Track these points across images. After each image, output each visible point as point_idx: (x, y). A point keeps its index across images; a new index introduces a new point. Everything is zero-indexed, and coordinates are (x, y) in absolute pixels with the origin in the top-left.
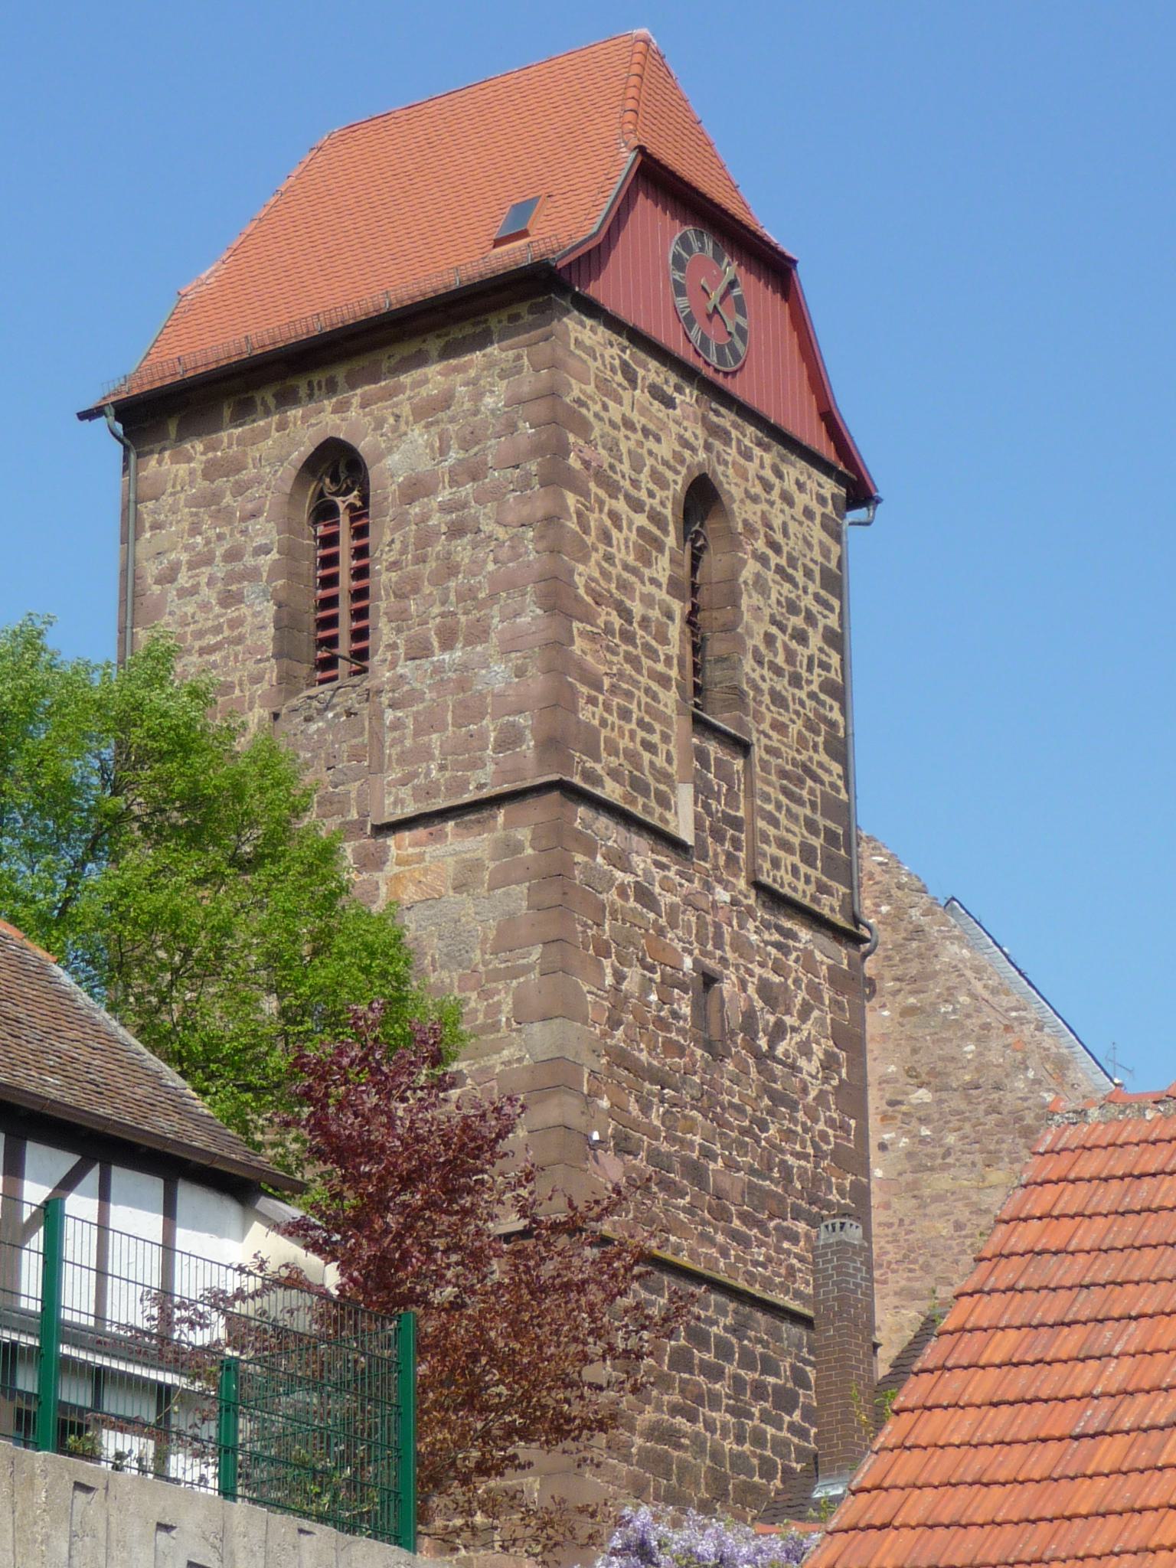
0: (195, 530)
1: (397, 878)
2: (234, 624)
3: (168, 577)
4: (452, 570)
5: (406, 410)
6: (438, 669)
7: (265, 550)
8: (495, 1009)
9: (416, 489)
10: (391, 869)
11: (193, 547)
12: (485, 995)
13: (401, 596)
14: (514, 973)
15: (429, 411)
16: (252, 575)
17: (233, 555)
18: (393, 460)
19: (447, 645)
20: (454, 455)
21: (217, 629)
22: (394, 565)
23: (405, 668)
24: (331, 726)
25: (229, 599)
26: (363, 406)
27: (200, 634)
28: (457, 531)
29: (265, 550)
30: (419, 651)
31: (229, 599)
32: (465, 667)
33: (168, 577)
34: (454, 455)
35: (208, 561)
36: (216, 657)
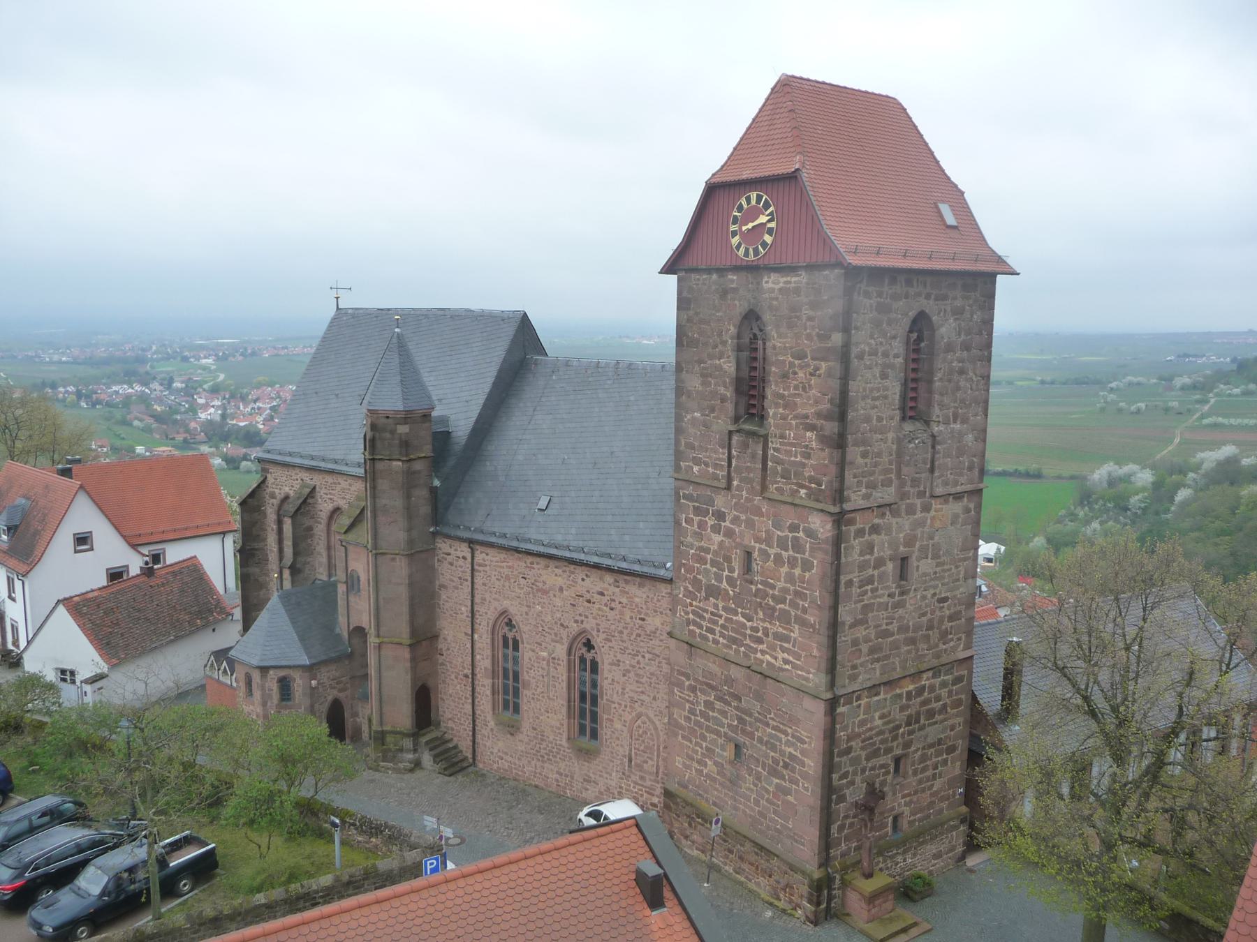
0: (872, 337)
1: (933, 518)
2: (886, 389)
3: (860, 357)
4: (958, 388)
5: (949, 309)
6: (952, 431)
7: (896, 356)
8: (959, 573)
9: (950, 348)
10: (933, 513)
11: (869, 344)
12: (957, 567)
13: (942, 395)
14: (965, 559)
15: (957, 312)
16: (892, 366)
17: (886, 355)
18: (943, 330)
19: (955, 422)
20: (963, 337)
21: (878, 390)
22: (941, 379)
23: (942, 428)
24: (917, 447)
25: (884, 376)
26: (936, 300)
27: (872, 390)
28: (962, 372)
29: (896, 356)
30: (947, 423)
31: (884, 376)
32: (960, 432)
33: (860, 357)
34: (963, 337)
35: (876, 355)
36: (877, 403)
